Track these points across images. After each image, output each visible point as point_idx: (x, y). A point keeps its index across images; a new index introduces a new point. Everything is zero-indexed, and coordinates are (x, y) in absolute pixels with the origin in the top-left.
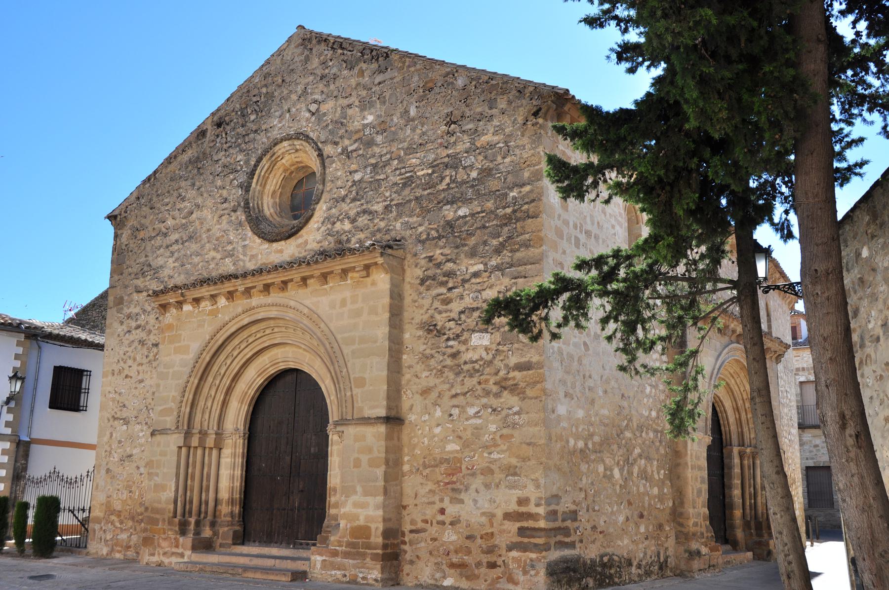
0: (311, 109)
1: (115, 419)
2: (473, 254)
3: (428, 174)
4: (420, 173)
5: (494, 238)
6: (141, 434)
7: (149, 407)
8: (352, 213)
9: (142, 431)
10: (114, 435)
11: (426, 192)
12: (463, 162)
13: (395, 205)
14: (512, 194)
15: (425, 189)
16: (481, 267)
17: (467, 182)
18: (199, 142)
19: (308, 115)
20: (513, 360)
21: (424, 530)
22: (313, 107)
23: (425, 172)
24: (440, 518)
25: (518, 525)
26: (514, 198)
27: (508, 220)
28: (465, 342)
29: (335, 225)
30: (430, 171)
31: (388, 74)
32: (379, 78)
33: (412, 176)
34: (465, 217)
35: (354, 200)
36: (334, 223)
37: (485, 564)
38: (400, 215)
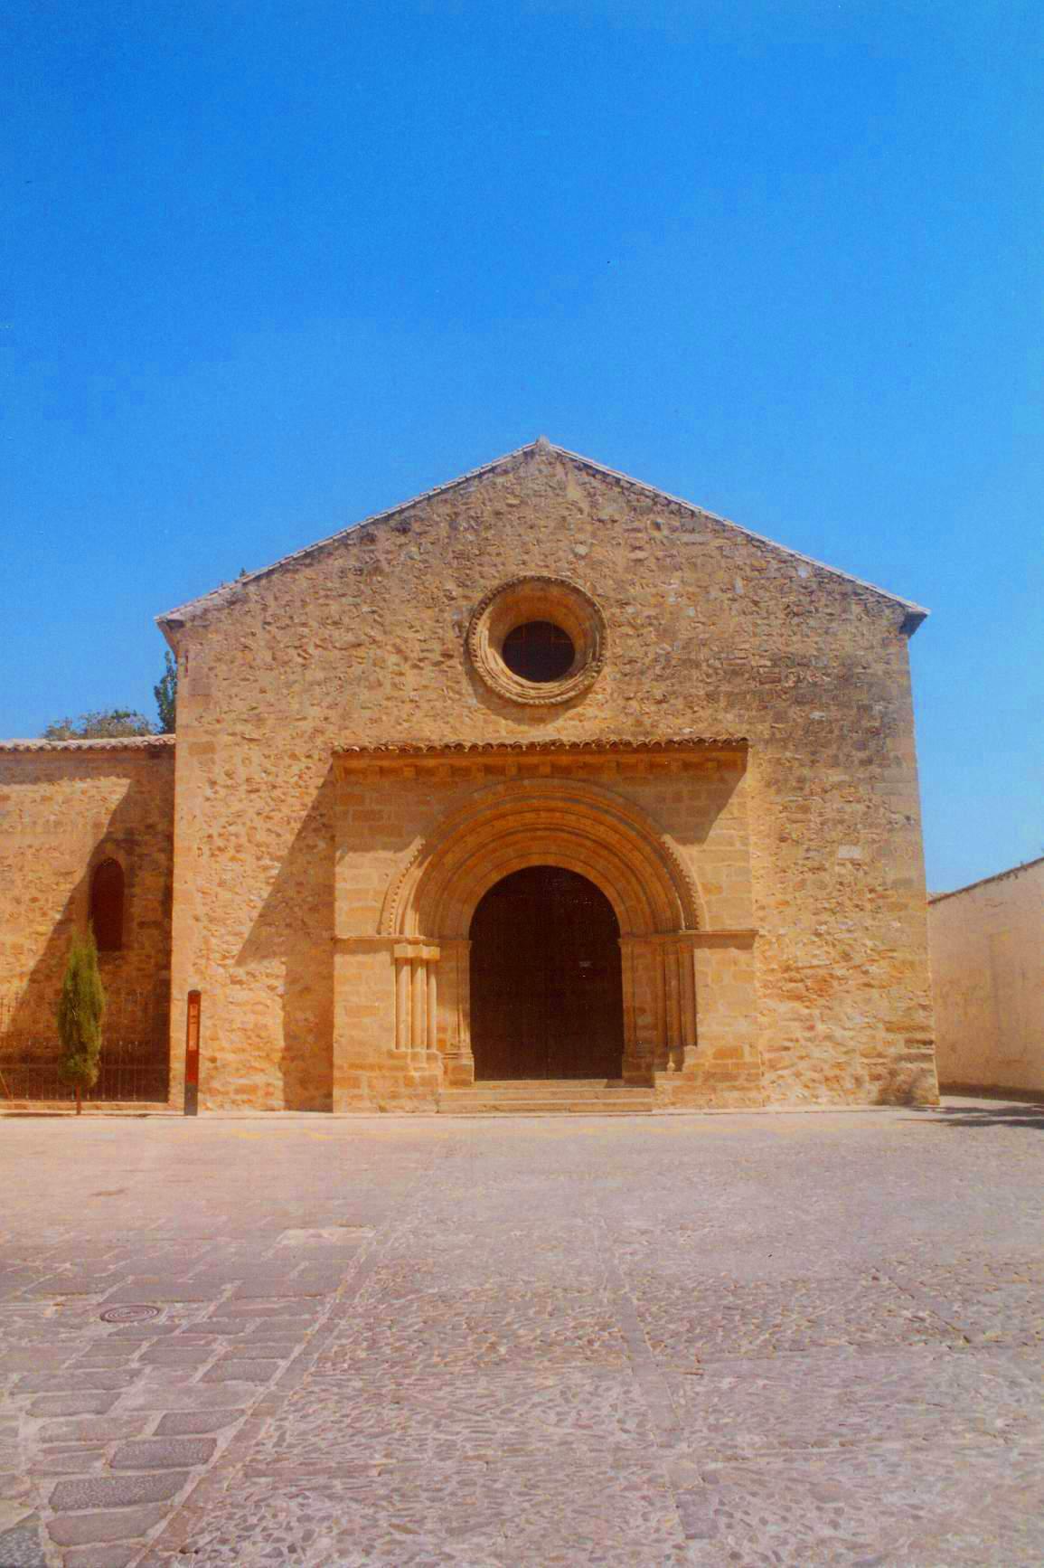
0: (576, 550)
1: (211, 920)
2: (835, 763)
3: (765, 666)
4: (753, 663)
5: (859, 750)
6: (277, 940)
7: (291, 903)
8: (658, 695)
9: (281, 936)
10: (214, 941)
11: (767, 686)
12: (814, 662)
13: (729, 694)
14: (878, 708)
15: (761, 683)
16: (846, 778)
17: (822, 685)
18: (366, 548)
19: (571, 557)
20: (892, 875)
21: (787, 1049)
22: (582, 550)
23: (763, 662)
24: (808, 1034)
25: (908, 1035)
26: (880, 712)
27: (875, 733)
28: (832, 853)
29: (631, 702)
30: (769, 663)
31: (696, 537)
32: (686, 538)
33: (744, 664)
34: (820, 722)
35: (659, 678)
36: (630, 699)
37: (867, 1078)
38: (731, 705)
